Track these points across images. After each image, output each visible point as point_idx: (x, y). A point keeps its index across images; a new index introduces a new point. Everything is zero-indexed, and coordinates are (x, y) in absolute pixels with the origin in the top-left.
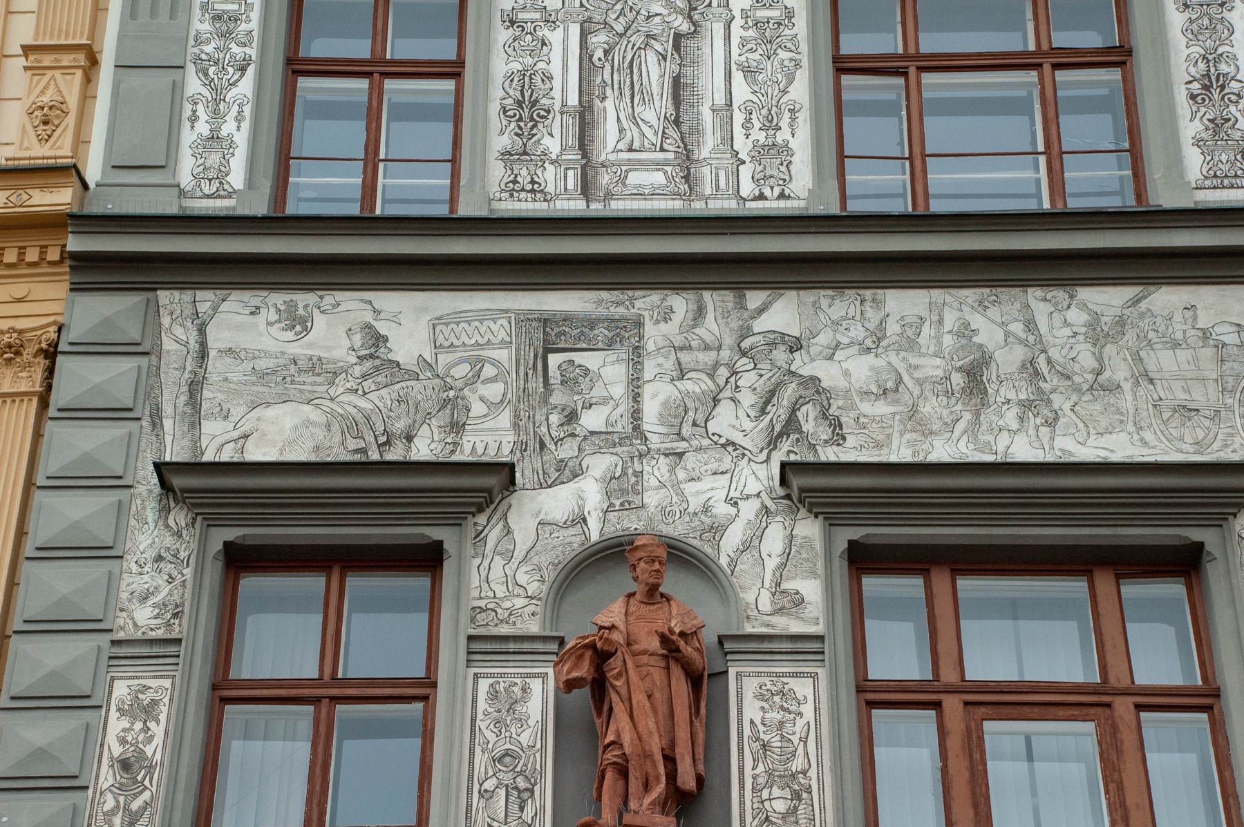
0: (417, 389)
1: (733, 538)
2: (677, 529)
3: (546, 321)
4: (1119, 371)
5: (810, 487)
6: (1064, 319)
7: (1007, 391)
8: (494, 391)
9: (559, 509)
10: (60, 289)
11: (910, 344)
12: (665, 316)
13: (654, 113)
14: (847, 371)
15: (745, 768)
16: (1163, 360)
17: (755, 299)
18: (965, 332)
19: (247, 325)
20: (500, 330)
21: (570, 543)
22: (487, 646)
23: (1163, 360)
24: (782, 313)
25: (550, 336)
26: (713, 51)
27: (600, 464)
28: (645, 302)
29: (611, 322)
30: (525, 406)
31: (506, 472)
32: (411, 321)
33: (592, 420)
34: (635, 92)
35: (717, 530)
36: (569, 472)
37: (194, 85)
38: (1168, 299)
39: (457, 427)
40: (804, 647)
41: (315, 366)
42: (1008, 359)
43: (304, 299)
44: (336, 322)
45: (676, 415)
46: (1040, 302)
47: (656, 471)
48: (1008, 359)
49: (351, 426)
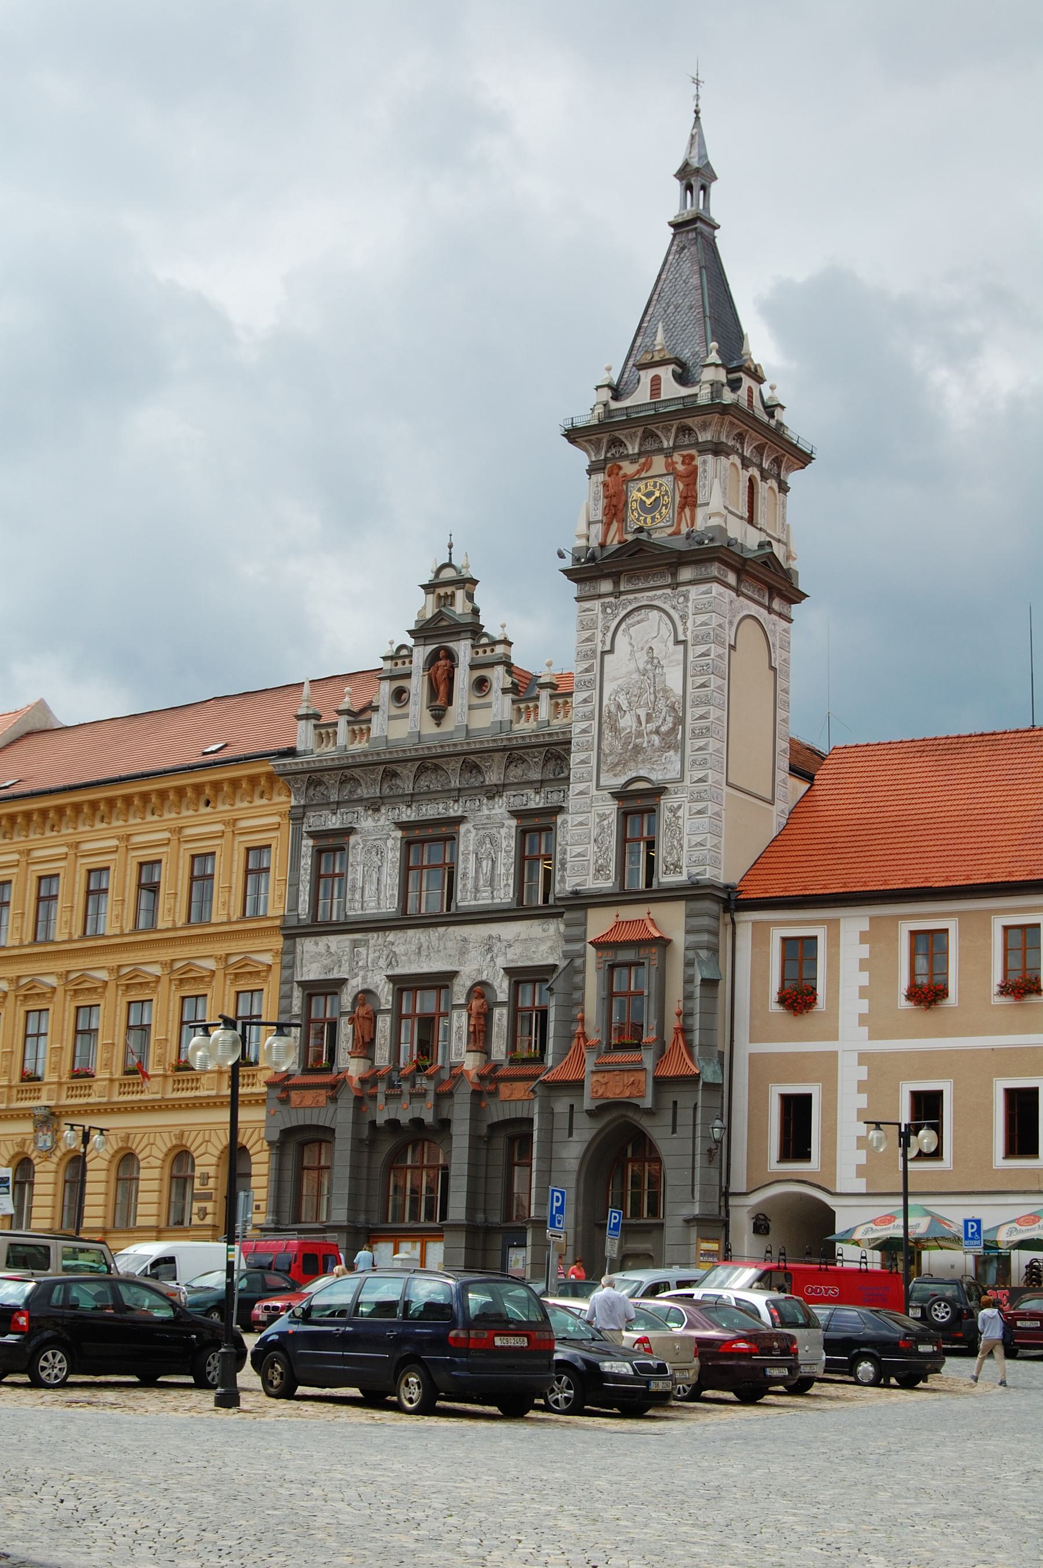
0: (335, 958)
1: (380, 988)
2: (371, 987)
3: (355, 941)
4: (441, 948)
5: (391, 978)
6: (435, 934)
7: (424, 953)
8: (346, 958)
9: (355, 984)
10: (282, 939)
11: (410, 943)
12: (374, 938)
13: (374, 887)
14: (399, 949)
15: (378, 1035)
16: (449, 944)
17: (387, 933)
18: (419, 939)
19: (308, 946)
20: (347, 943)
21: (356, 990)
22: (343, 1014)
23: (449, 944)
24: (391, 936)
25: (355, 944)
26: (385, 869)
27: (361, 973)
28: (370, 935)
29: (365, 940)
30: (351, 959)
31: (346, 980)
32: (334, 942)
33: (360, 964)
34: (371, 882)
35: (378, 987)
36: (357, 975)
37: (301, 888)
38: (452, 929)
39: (340, 966)
40: (387, 1011)
41: (320, 954)
42: (425, 945)
43: (318, 938)
44: (324, 940)
45: (373, 962)
46: (431, 931)
47: (370, 974)
48: (425, 945)
49: (325, 967)
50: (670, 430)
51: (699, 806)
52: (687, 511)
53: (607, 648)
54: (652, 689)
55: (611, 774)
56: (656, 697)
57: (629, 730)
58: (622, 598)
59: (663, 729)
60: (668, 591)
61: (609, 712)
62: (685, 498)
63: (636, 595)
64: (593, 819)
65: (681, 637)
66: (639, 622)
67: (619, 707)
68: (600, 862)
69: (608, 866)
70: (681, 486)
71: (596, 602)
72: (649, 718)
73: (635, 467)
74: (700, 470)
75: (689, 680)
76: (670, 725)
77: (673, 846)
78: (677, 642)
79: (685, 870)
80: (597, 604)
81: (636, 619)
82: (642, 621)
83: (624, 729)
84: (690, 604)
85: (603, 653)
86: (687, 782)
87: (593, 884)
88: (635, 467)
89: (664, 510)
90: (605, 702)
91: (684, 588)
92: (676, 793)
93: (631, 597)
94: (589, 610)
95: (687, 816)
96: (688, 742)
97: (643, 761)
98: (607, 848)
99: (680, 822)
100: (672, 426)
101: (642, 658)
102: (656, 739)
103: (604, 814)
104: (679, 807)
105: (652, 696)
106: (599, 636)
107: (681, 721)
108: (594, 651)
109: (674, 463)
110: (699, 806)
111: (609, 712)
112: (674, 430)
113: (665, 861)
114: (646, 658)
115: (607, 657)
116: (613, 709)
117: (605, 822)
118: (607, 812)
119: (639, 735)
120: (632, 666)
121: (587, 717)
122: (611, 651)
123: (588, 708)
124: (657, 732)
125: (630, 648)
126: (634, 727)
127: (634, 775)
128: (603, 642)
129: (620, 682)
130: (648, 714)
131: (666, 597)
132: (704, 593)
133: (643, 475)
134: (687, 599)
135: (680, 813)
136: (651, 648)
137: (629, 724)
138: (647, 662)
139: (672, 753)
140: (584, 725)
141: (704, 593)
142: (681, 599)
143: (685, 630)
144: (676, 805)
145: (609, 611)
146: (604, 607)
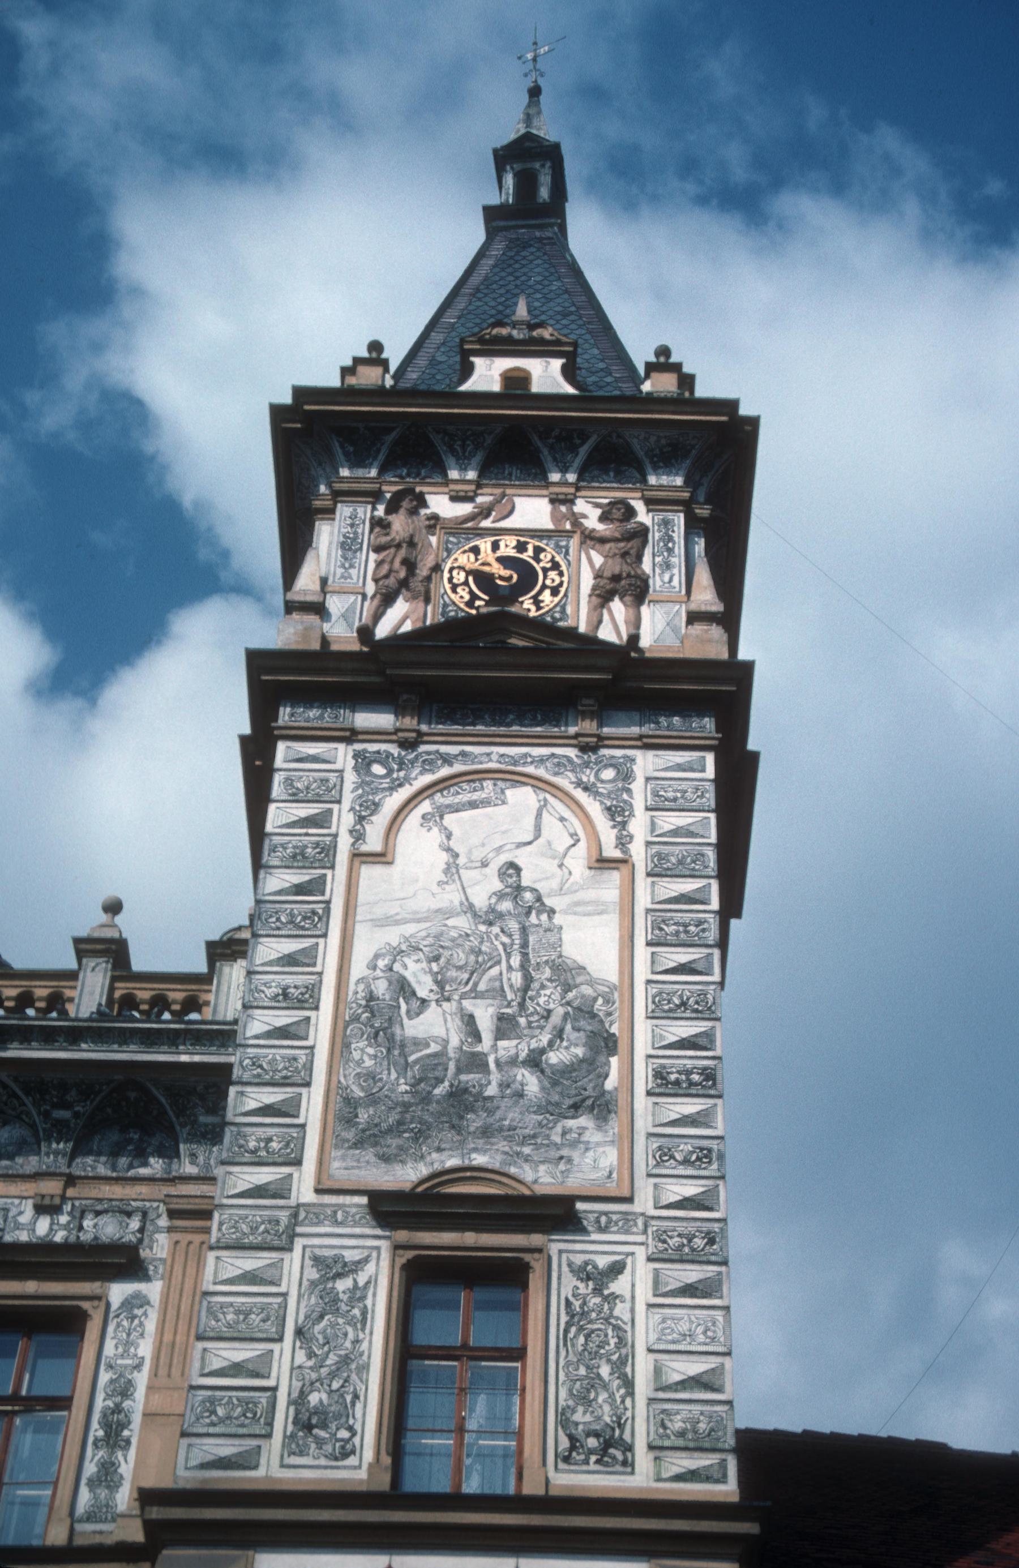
50: (574, 449)
51: (692, 1274)
52: (617, 606)
53: (373, 843)
54: (516, 961)
55: (369, 1154)
56: (528, 979)
57: (434, 1048)
58: (423, 748)
59: (553, 1058)
60: (572, 753)
61: (371, 997)
62: (616, 578)
63: (468, 748)
64: (294, 1268)
65: (611, 851)
66: (473, 805)
67: (403, 988)
68: (314, 1398)
69: (344, 1414)
70: (598, 560)
71: (341, 747)
72: (505, 1027)
73: (465, 509)
74: (655, 535)
75: (642, 953)
76: (580, 1051)
77: (594, 1381)
78: (602, 863)
79: (642, 1458)
80: (343, 755)
81: (465, 797)
82: (485, 803)
83: (420, 1043)
84: (637, 786)
85: (358, 857)
86: (644, 1203)
87: (275, 1467)
88: (465, 509)
89: (546, 596)
90: (358, 969)
91: (618, 753)
92: (602, 1230)
93: (453, 750)
94: (315, 759)
95: (644, 1294)
96: (641, 1102)
97: (486, 1132)
98: (345, 1361)
99: (621, 1310)
100: (584, 438)
101: (483, 889)
102: (532, 1083)
103: (337, 1259)
104: (616, 1269)
105: (517, 978)
106: (344, 820)
107: (605, 1044)
108: (327, 853)
109: (576, 520)
110: (692, 1274)
111: (371, 997)
112: (584, 451)
113: (564, 1420)
114: (498, 885)
115: (368, 873)
116: (381, 988)
117: (343, 1285)
118: (350, 1256)
119: (476, 1062)
120: (452, 897)
121: (285, 998)
122: (382, 858)
123: (295, 979)
124: (535, 1061)
125: (444, 856)
126: (454, 1041)
127: (452, 1162)
128: (358, 836)
129: (410, 929)
130: (501, 1018)
131: (561, 765)
132: (679, 767)
133: (486, 523)
134: (626, 776)
135: (619, 1286)
136: (512, 865)
137: (440, 1031)
138: (501, 896)
139: (584, 1121)
140: (283, 1018)
141: (679, 767)
142: (609, 774)
143: (623, 842)
144: (602, 1262)
145: (378, 769)
146: (364, 763)
